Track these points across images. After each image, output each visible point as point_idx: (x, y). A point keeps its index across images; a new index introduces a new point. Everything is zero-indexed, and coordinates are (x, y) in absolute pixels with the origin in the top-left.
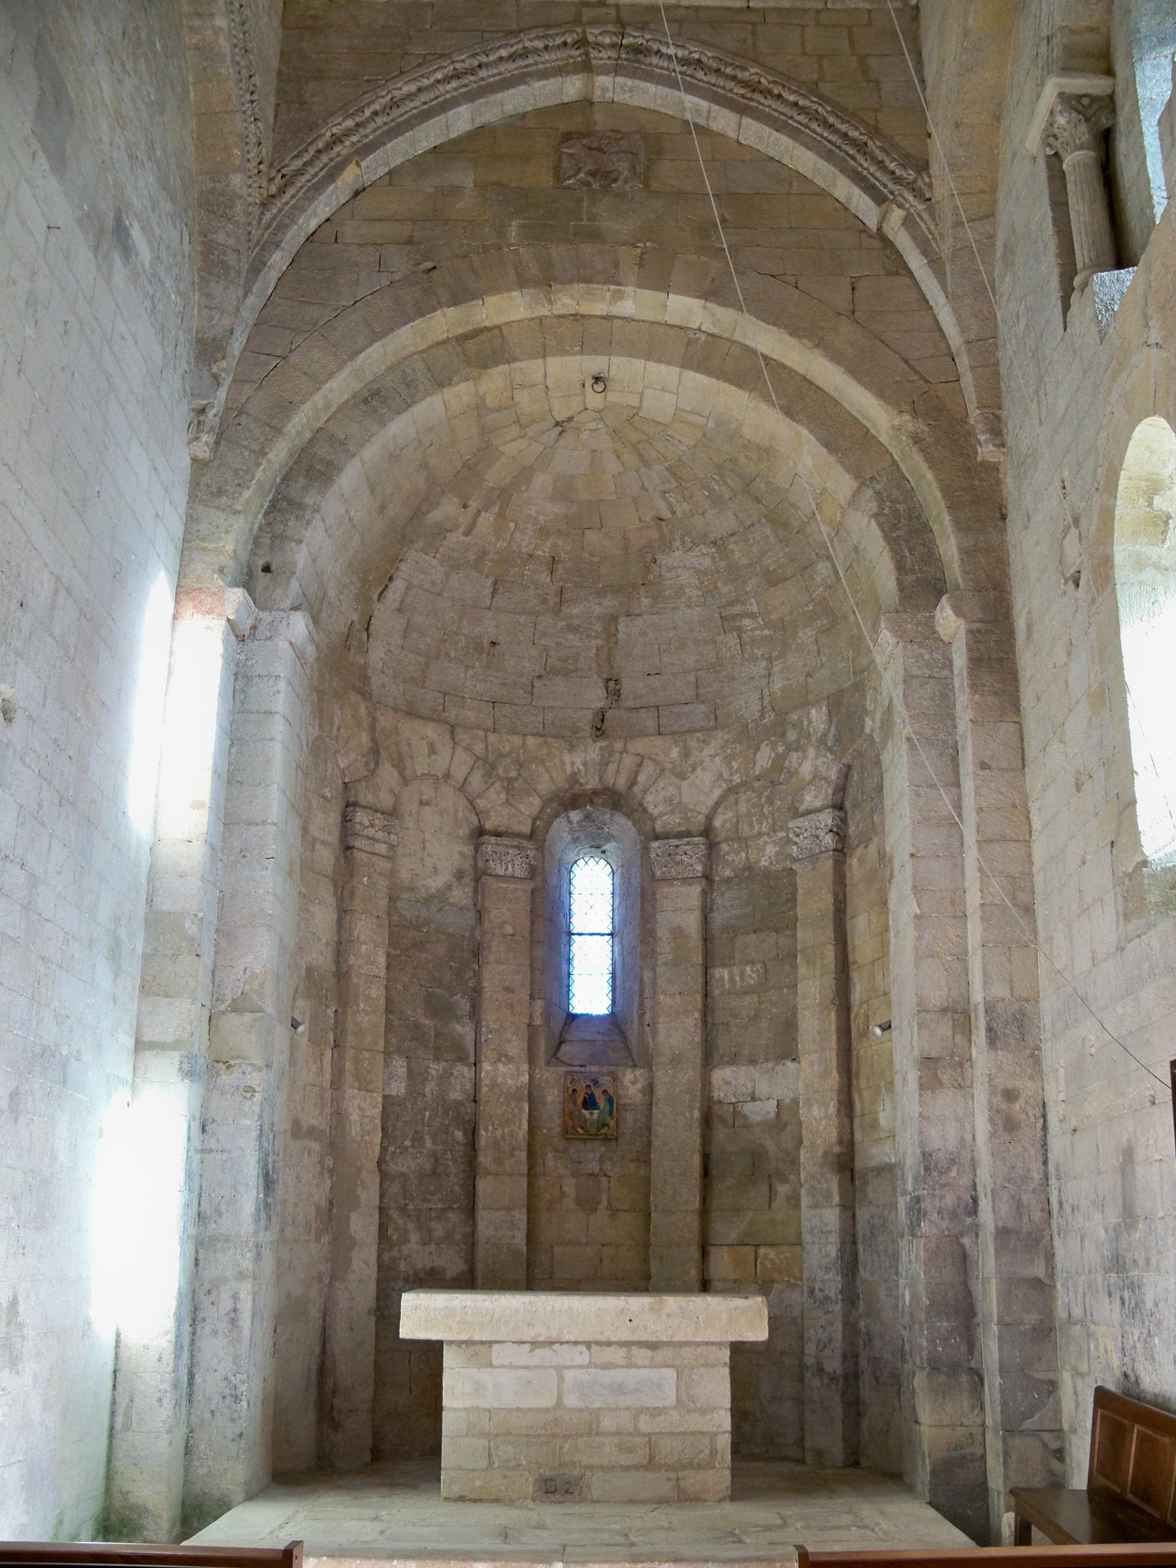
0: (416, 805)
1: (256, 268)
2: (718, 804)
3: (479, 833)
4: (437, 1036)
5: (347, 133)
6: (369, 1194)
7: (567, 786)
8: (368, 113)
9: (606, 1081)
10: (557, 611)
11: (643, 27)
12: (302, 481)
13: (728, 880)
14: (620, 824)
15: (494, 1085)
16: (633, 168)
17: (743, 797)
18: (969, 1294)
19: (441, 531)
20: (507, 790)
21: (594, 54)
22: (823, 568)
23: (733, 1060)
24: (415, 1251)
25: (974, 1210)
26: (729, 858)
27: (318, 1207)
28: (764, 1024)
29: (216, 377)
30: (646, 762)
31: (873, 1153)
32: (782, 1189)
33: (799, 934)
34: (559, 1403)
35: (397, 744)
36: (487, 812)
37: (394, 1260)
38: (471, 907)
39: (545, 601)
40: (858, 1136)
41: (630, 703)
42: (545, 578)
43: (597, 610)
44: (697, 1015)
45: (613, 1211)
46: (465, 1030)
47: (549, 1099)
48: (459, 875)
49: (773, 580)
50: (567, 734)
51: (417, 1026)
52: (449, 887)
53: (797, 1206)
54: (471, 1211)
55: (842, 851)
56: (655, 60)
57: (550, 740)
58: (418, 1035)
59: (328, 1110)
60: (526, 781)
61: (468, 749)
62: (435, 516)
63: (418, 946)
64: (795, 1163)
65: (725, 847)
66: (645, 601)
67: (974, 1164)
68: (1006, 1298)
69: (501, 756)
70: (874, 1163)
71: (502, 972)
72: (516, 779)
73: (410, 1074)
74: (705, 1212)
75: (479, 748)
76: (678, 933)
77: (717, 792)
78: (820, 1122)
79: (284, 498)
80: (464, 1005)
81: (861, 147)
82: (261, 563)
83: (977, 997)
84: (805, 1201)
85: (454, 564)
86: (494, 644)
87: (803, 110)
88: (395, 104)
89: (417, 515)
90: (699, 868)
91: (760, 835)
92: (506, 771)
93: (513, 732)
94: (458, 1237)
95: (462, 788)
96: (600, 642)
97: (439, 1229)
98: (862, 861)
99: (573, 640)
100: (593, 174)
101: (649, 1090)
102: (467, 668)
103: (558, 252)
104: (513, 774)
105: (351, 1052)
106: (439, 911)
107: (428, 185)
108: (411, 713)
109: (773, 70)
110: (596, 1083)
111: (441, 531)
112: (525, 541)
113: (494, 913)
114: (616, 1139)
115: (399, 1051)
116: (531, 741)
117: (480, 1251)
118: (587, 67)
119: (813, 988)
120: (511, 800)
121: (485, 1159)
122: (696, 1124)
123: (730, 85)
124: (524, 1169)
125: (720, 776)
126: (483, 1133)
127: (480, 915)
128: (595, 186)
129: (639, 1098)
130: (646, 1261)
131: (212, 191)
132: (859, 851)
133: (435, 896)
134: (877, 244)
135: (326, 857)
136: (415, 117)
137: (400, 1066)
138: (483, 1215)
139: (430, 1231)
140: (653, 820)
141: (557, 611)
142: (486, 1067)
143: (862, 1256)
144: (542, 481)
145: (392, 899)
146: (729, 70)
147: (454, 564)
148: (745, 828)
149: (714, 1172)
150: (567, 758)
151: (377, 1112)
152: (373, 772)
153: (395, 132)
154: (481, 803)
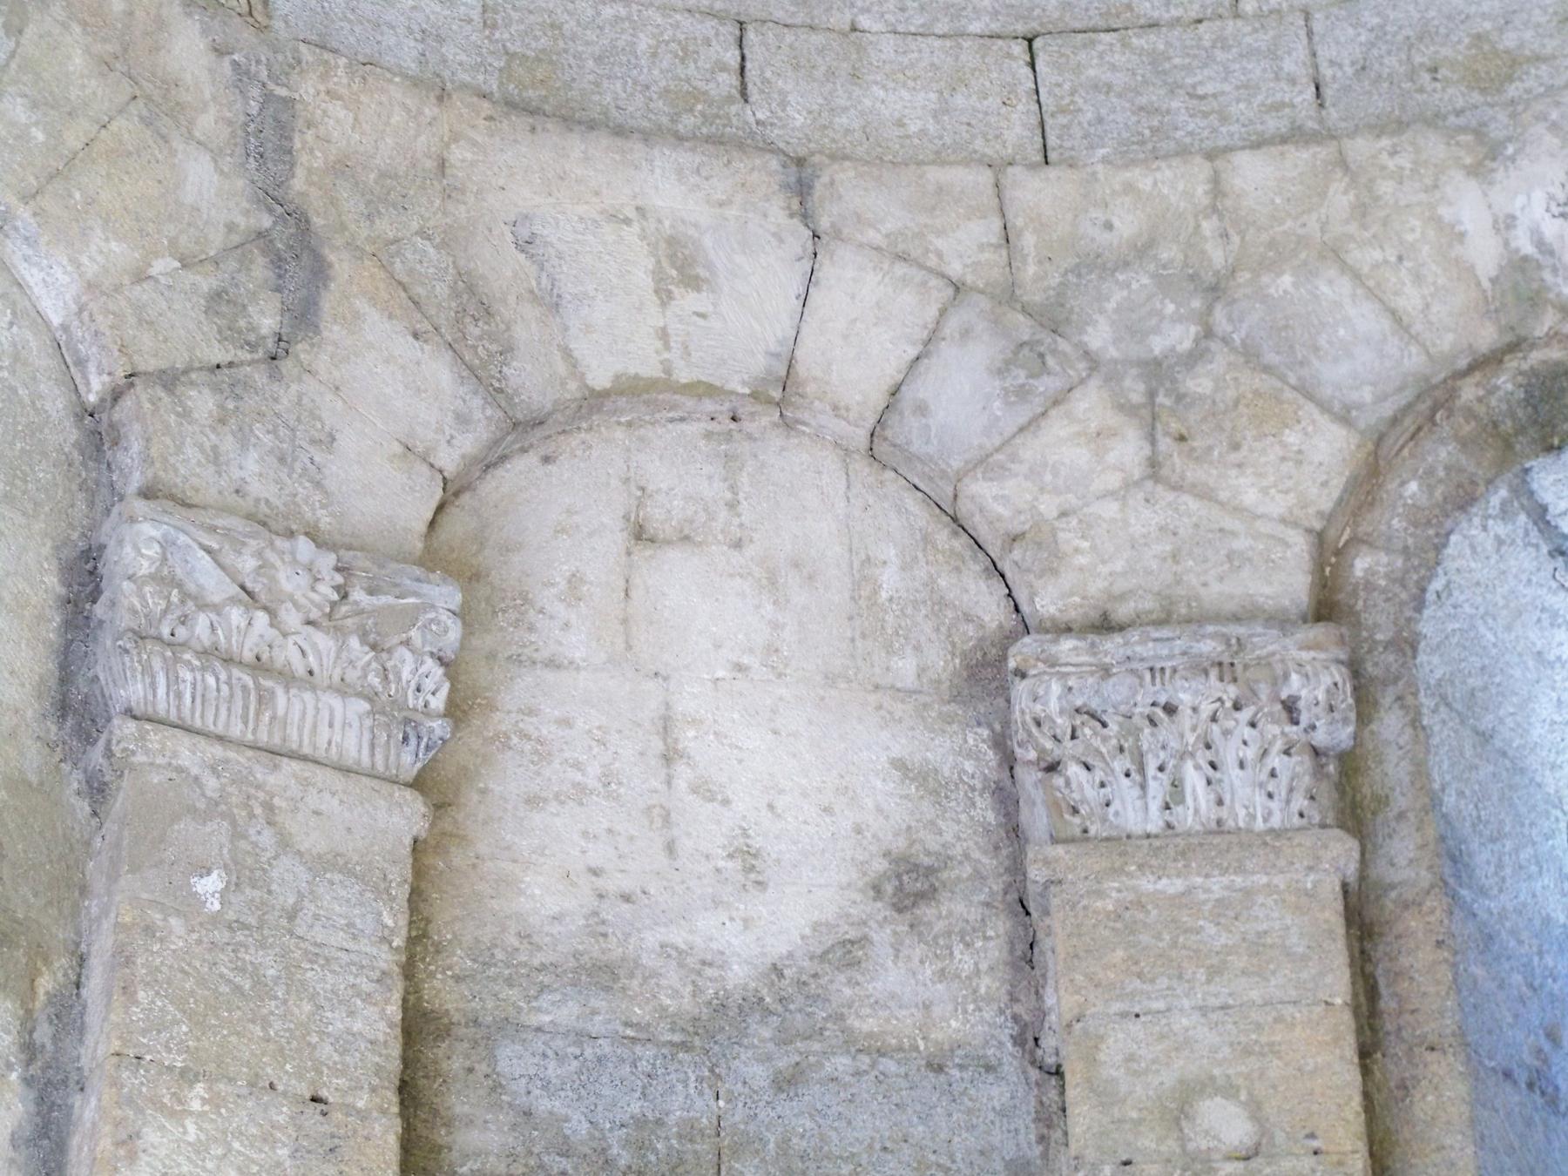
0: (615, 539)
7: (1487, 337)
20: (1149, 419)
38: (1010, 1058)
48: (909, 885)
50: (1455, 96)
52: (847, 952)
57: (1360, 148)
60: (1250, 355)
69: (1096, 266)
72: (1195, 357)
75: (966, 245)
92: (1134, 331)
93: (1152, 145)
95: (879, 445)
104: (1178, 337)
106: (786, 1083)
113: (1118, 1042)
116: (1254, 175)
120: (1177, 463)
133: (753, 1004)
150: (1468, 206)
154: (995, 501)
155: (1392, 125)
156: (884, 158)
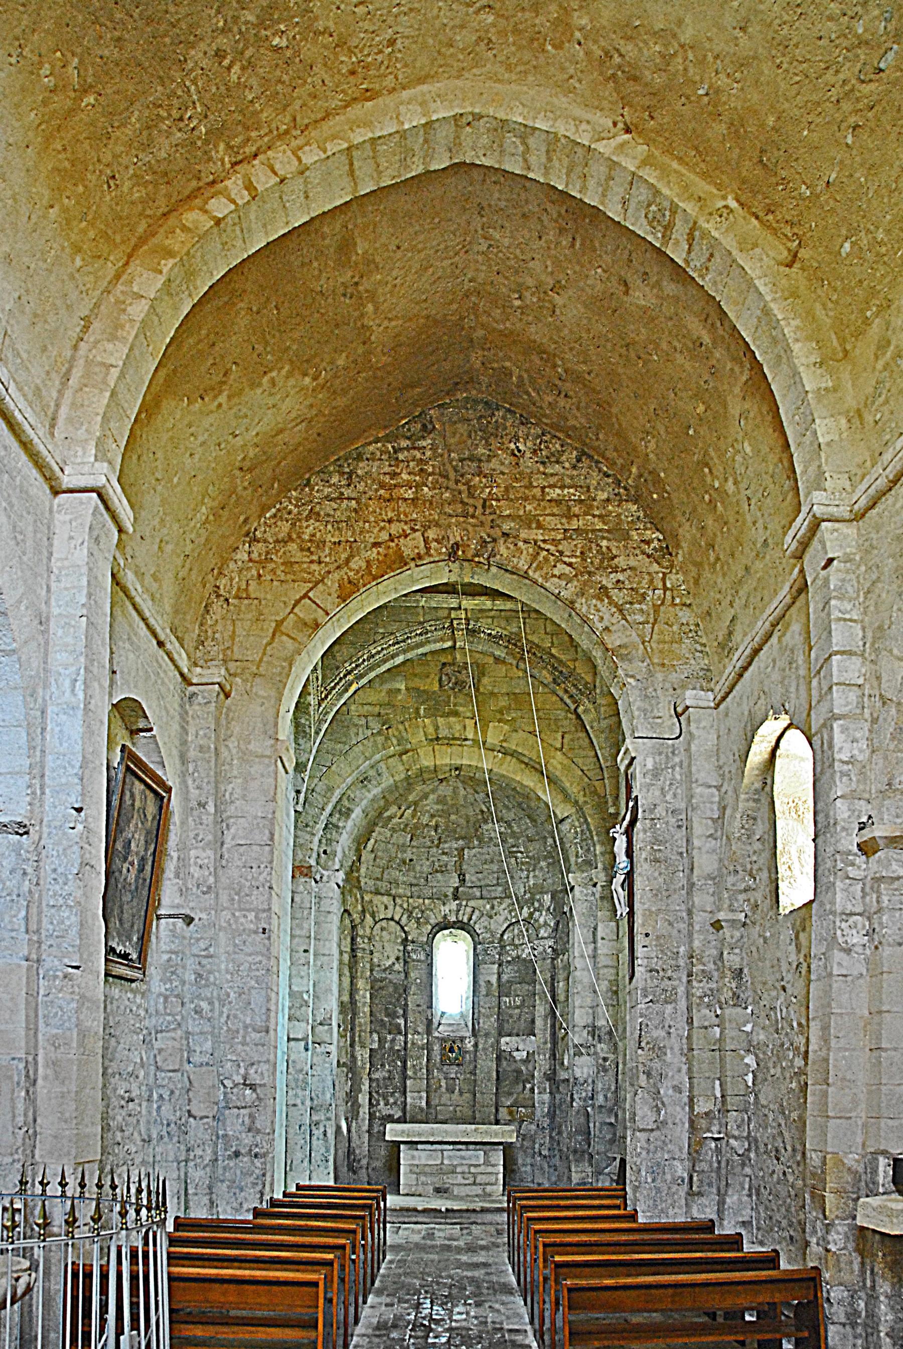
6: (365, 1087)
10: (438, 847)
19: (390, 818)
24: (383, 1109)
42: (433, 833)
48: (398, 959)
61: (401, 906)
66: (476, 842)
73: (379, 1041)
75: (405, 906)
77: (506, 925)
80: (401, 1012)
93: (419, 897)
97: (391, 1100)
99: (445, 858)
101: (476, 1045)
108: (377, 893)
116: (427, 901)
125: (506, 919)
137: (375, 1037)
141: (438, 847)
142: (410, 1036)
147: (393, 830)
150: (442, 908)
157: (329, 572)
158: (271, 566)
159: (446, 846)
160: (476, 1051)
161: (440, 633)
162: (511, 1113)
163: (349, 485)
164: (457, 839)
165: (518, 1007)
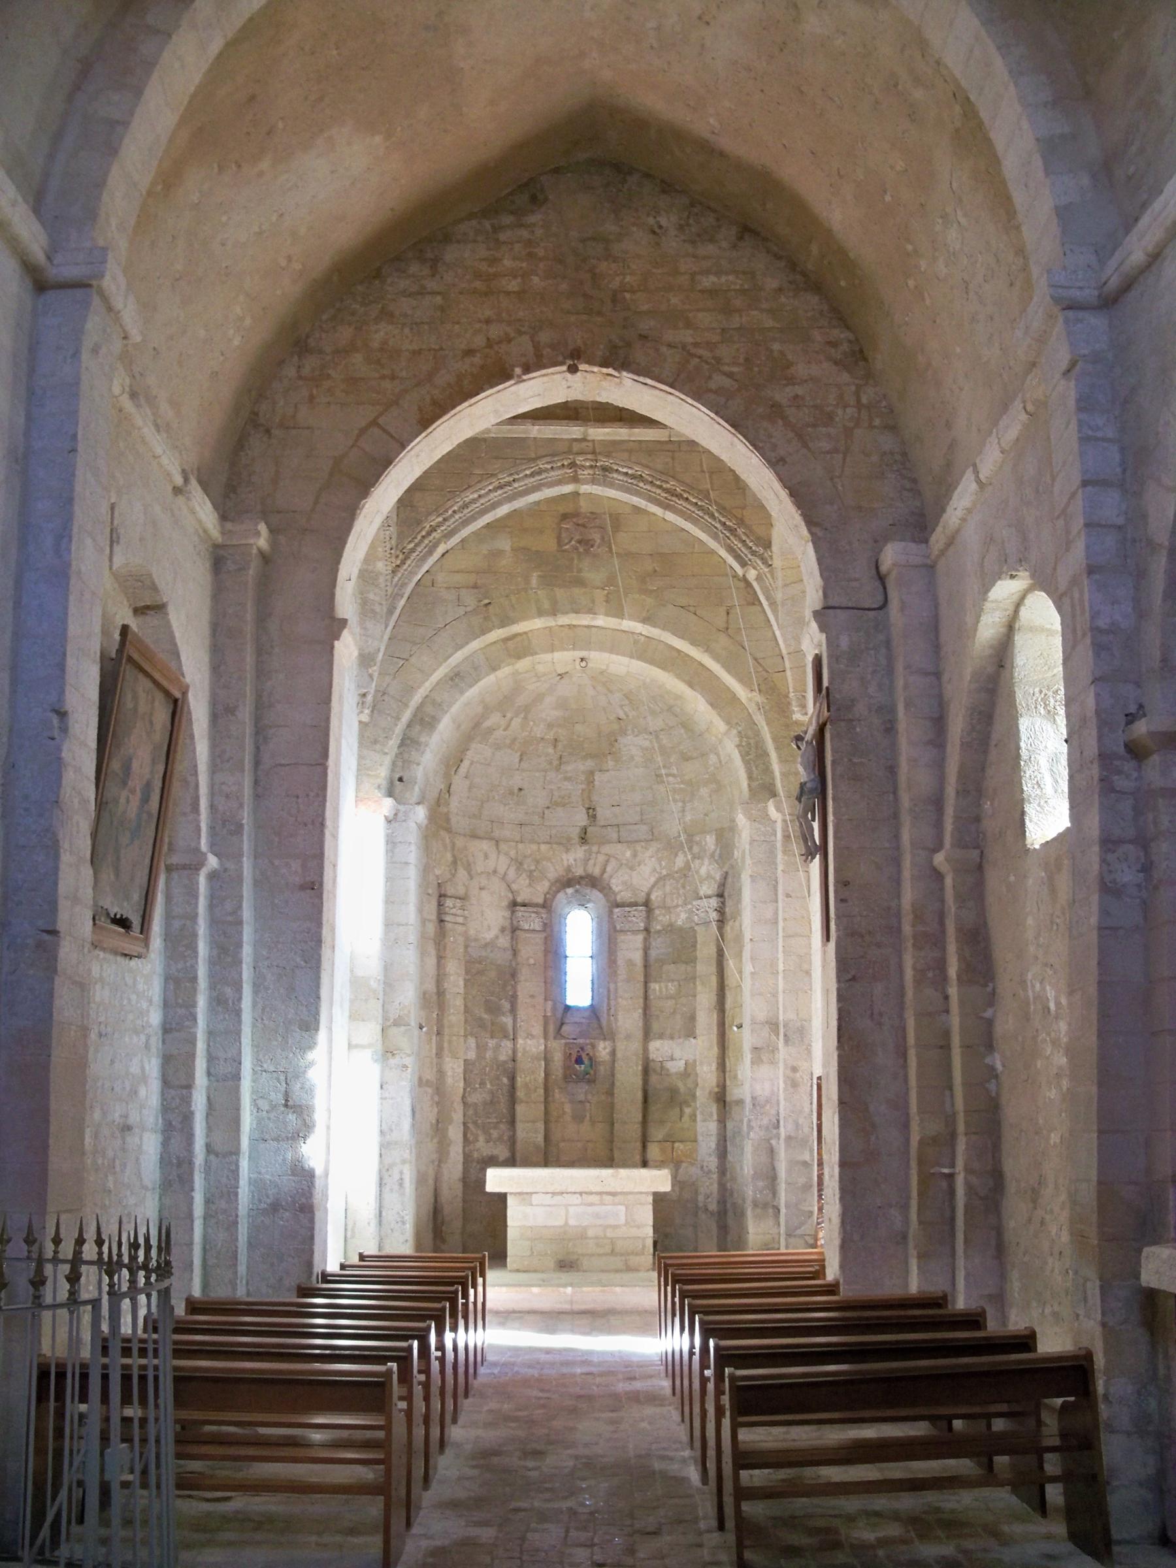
1: (390, 612)
2: (653, 886)
3: (514, 904)
4: (492, 1024)
5: (439, 525)
6: (458, 1116)
8: (450, 512)
9: (588, 1049)
10: (558, 769)
11: (608, 455)
12: (418, 728)
13: (659, 932)
14: (596, 894)
15: (525, 1051)
16: (603, 538)
17: (668, 883)
18: (774, 1169)
19: (491, 730)
21: (580, 472)
22: (713, 759)
23: (661, 1036)
24: (483, 1147)
25: (777, 1127)
26: (660, 918)
27: (432, 1124)
28: (678, 1017)
29: (371, 676)
30: (612, 859)
31: (734, 1093)
32: (687, 1111)
33: (698, 968)
34: (566, 1223)
35: (466, 856)
36: (518, 892)
37: (471, 1151)
39: (551, 763)
40: (728, 1083)
41: (602, 823)
42: (551, 750)
43: (582, 768)
44: (640, 1011)
45: (593, 1123)
46: (507, 1020)
47: (556, 1058)
48: (503, 930)
49: (686, 758)
50: (564, 841)
51: (481, 1019)
52: (497, 937)
53: (695, 1121)
54: (512, 1122)
55: (721, 922)
56: (615, 475)
58: (481, 1024)
59: (435, 1070)
61: (506, 854)
62: (487, 724)
63: (480, 973)
64: (694, 1096)
65: (657, 912)
66: (611, 763)
67: (778, 1104)
68: (789, 1171)
70: (735, 1098)
71: (528, 986)
73: (478, 1047)
74: (645, 1122)
76: (630, 963)
77: (653, 880)
78: (707, 1074)
79: (409, 738)
80: (506, 1005)
81: (732, 531)
82: (397, 776)
83: (781, 1018)
84: (699, 1118)
85: (498, 747)
86: (520, 789)
87: (701, 508)
88: (465, 506)
89: (477, 725)
90: (642, 925)
91: (677, 906)
93: (532, 841)
94: (505, 1138)
95: (503, 878)
96: (583, 786)
98: (732, 928)
99: (567, 785)
100: (580, 542)
101: (613, 1053)
102: (505, 805)
103: (560, 593)
104: (533, 868)
105: (446, 1038)
107: (485, 549)
108: (474, 836)
109: (682, 482)
110: (582, 1049)
111: (491, 730)
112: (539, 731)
114: (594, 1081)
115: (471, 1034)
116: (543, 847)
117: (519, 1146)
118: (575, 479)
119: (705, 998)
121: (520, 1094)
122: (640, 1073)
123: (658, 491)
124: (542, 1099)
125: (655, 870)
126: (519, 1079)
127: (515, 953)
128: (581, 550)
129: (607, 1058)
130: (611, 1150)
131: (366, 570)
132: (731, 923)
134: (742, 585)
135: (431, 928)
136: (477, 513)
137: (472, 1042)
138: (520, 1126)
139: (490, 1135)
140: (615, 894)
141: (558, 769)
142: (520, 1041)
143: (729, 1148)
144: (549, 700)
145: (466, 947)
146: (658, 483)
148: (669, 902)
149: (650, 1100)
150: (564, 856)
151: (461, 1070)
152: (454, 875)
153: (466, 523)
154: (514, 887)
155: (557, 843)
156: (506, 841)
157: (406, 391)
158: (327, 384)
159: (569, 768)
160: (614, 1061)
161: (560, 472)
162: (663, 1151)
163: (433, 276)
164: (585, 758)
165: (671, 997)
